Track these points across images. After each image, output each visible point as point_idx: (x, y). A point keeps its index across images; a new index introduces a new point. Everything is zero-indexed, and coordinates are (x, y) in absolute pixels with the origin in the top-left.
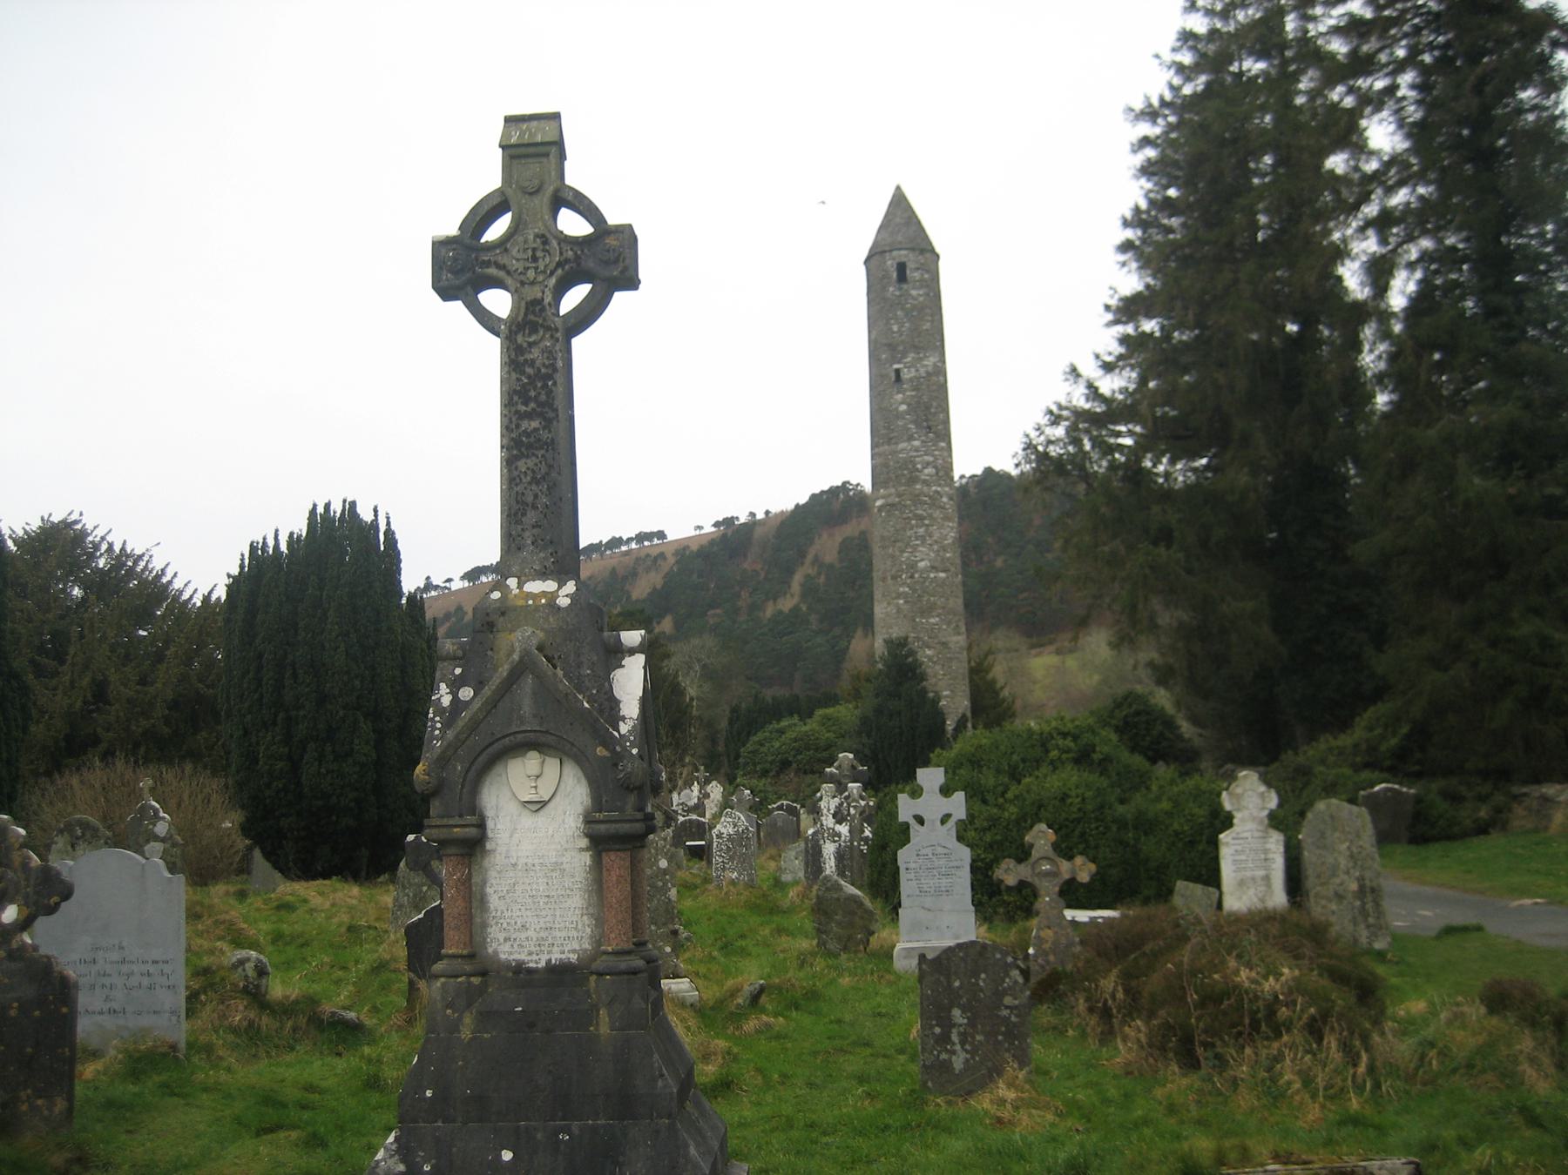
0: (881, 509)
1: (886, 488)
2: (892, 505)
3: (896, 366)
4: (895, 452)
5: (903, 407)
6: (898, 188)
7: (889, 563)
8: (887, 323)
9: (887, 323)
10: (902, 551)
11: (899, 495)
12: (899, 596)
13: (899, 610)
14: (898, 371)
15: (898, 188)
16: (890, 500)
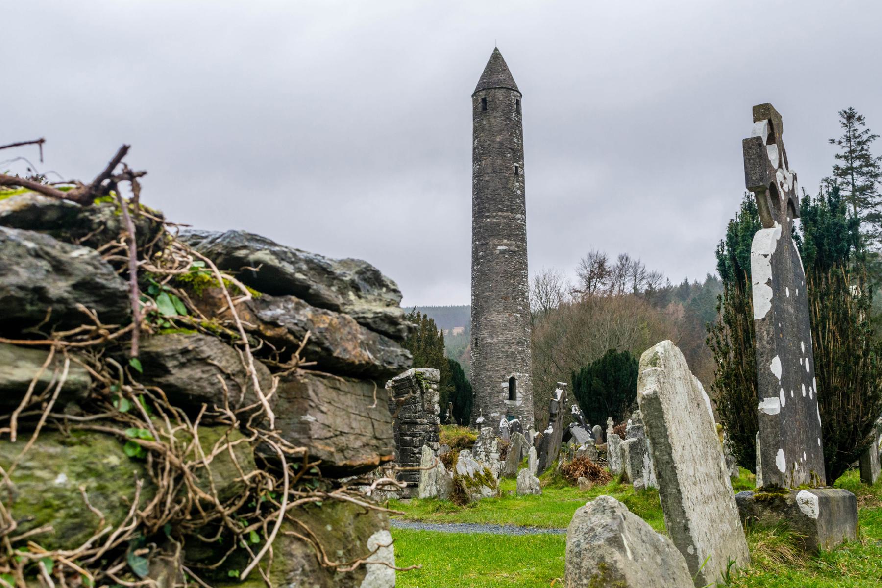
0: (503, 252)
1: (509, 240)
2: (514, 252)
3: (516, 164)
4: (514, 218)
5: (519, 192)
6: (496, 49)
7: (510, 288)
8: (511, 135)
9: (511, 135)
10: (519, 283)
11: (517, 246)
12: (517, 311)
13: (517, 321)
14: (516, 167)
15: (496, 49)
16: (512, 248)
